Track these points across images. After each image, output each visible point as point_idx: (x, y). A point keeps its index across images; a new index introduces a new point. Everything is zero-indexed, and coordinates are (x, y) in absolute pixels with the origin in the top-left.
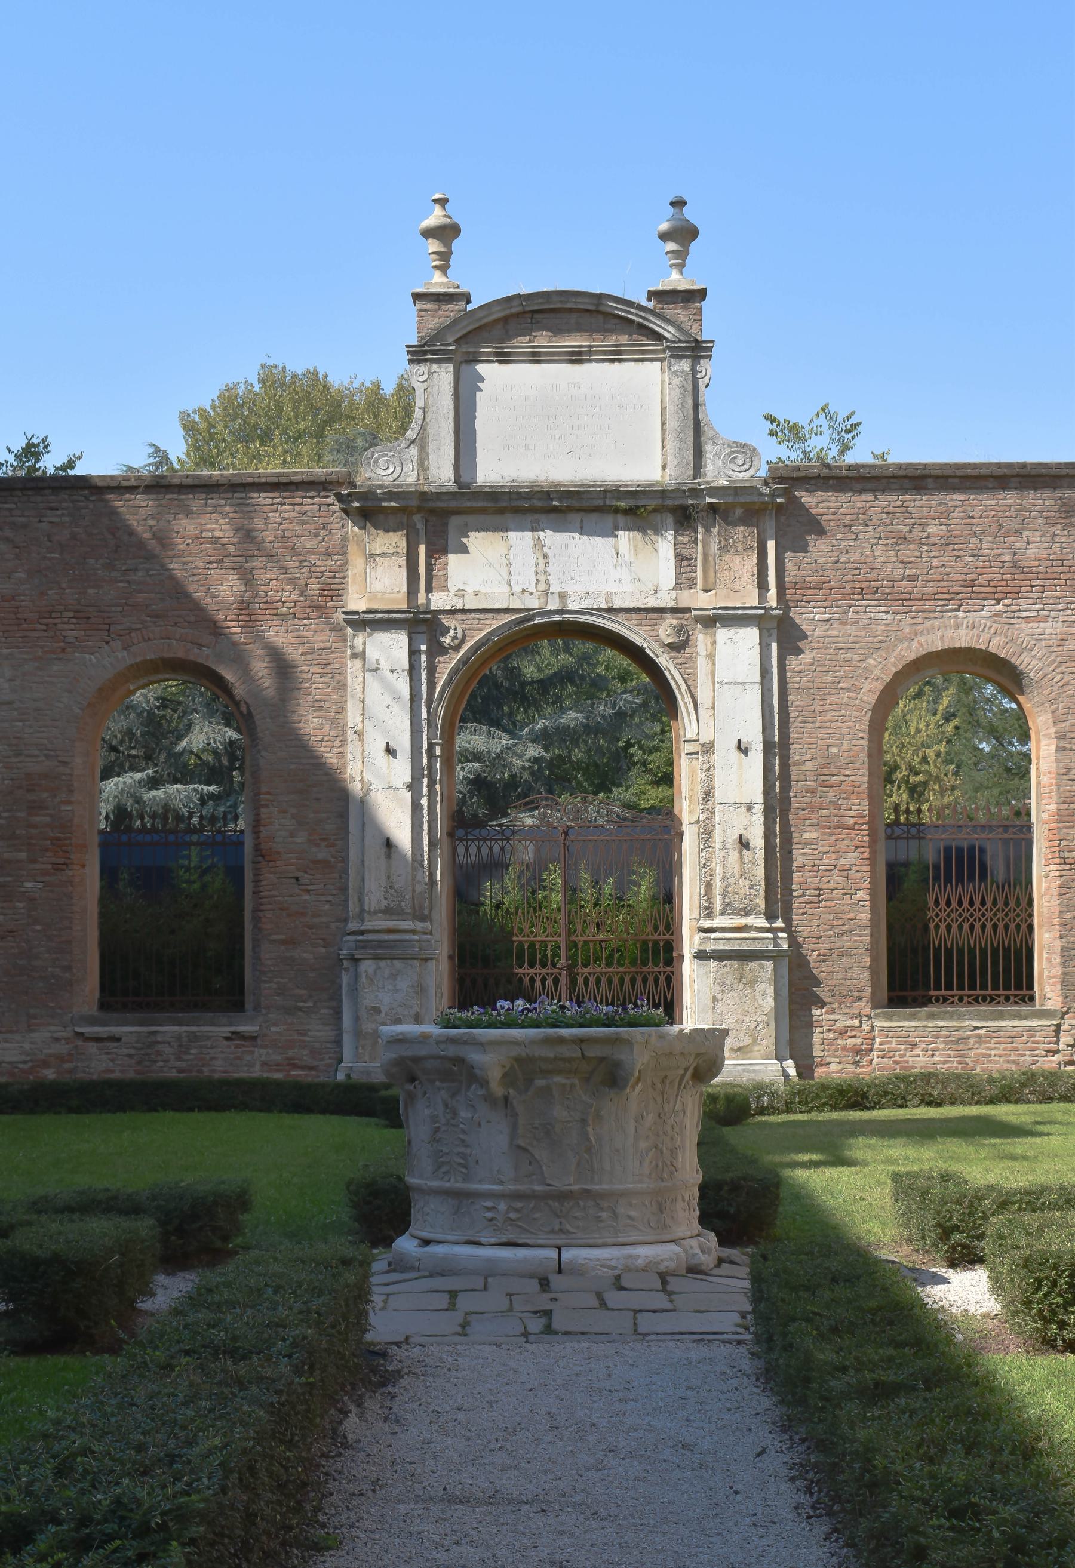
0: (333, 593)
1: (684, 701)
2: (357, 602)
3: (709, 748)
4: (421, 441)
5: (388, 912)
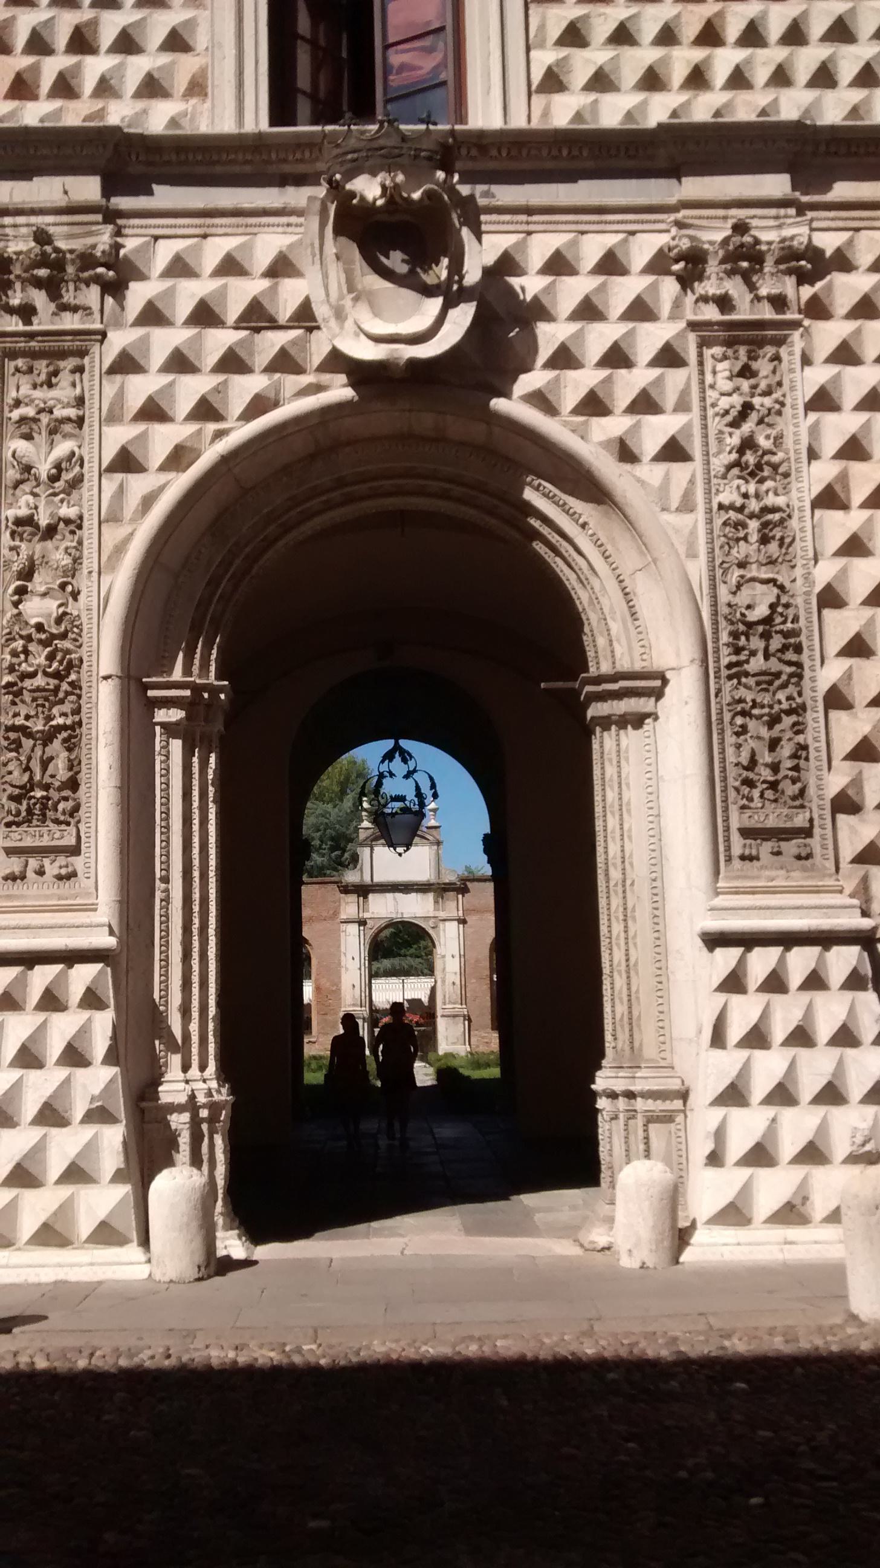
0: (336, 913)
1: (437, 943)
2: (343, 916)
3: (444, 957)
4: (361, 870)
5: (354, 1005)
